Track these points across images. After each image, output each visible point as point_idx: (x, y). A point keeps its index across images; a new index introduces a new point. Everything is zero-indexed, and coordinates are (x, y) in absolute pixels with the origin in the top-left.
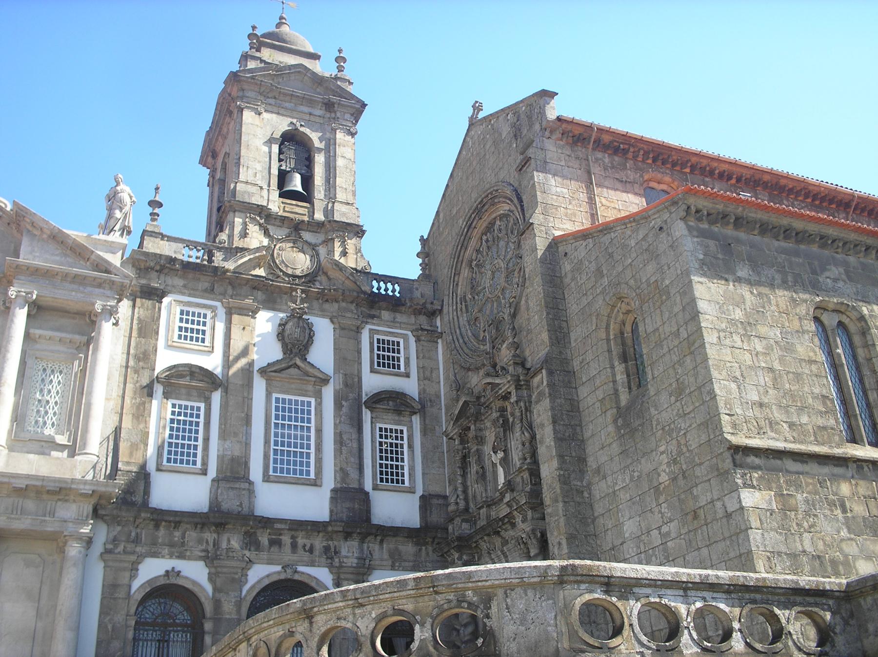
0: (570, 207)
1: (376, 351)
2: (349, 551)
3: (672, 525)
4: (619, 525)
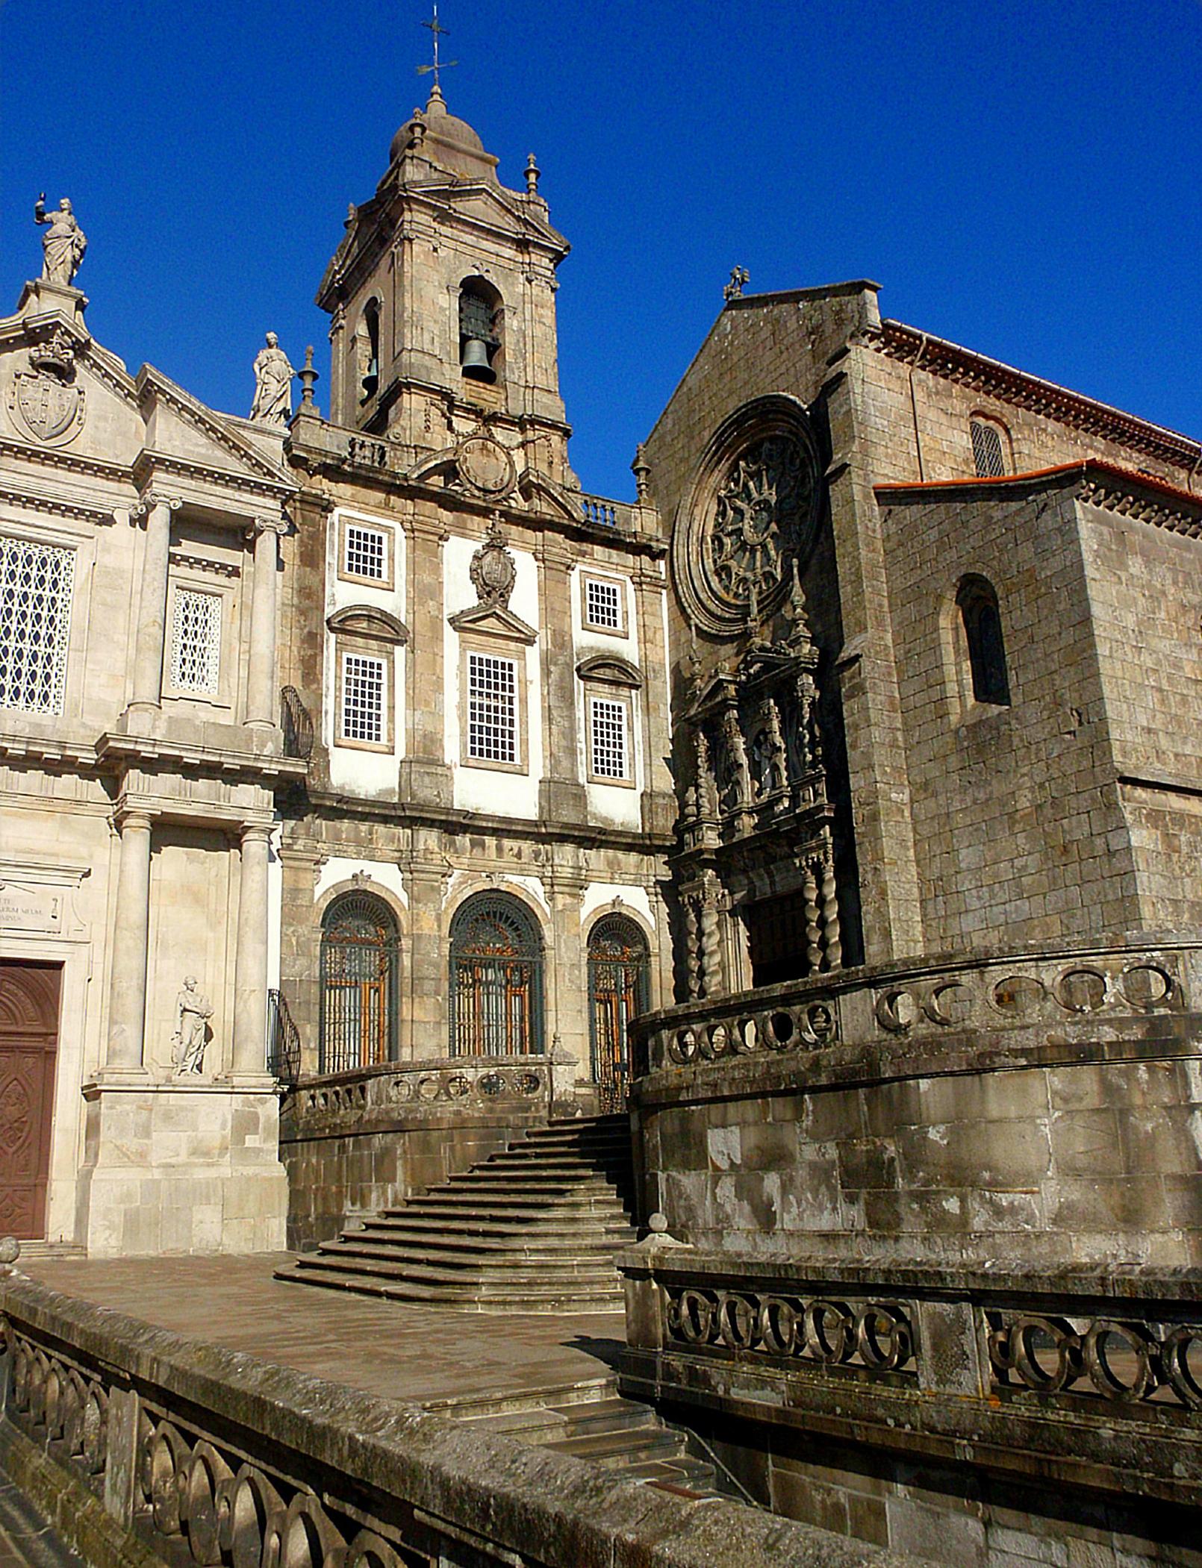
0: (890, 444)
1: (588, 602)
2: (566, 855)
3: (1030, 858)
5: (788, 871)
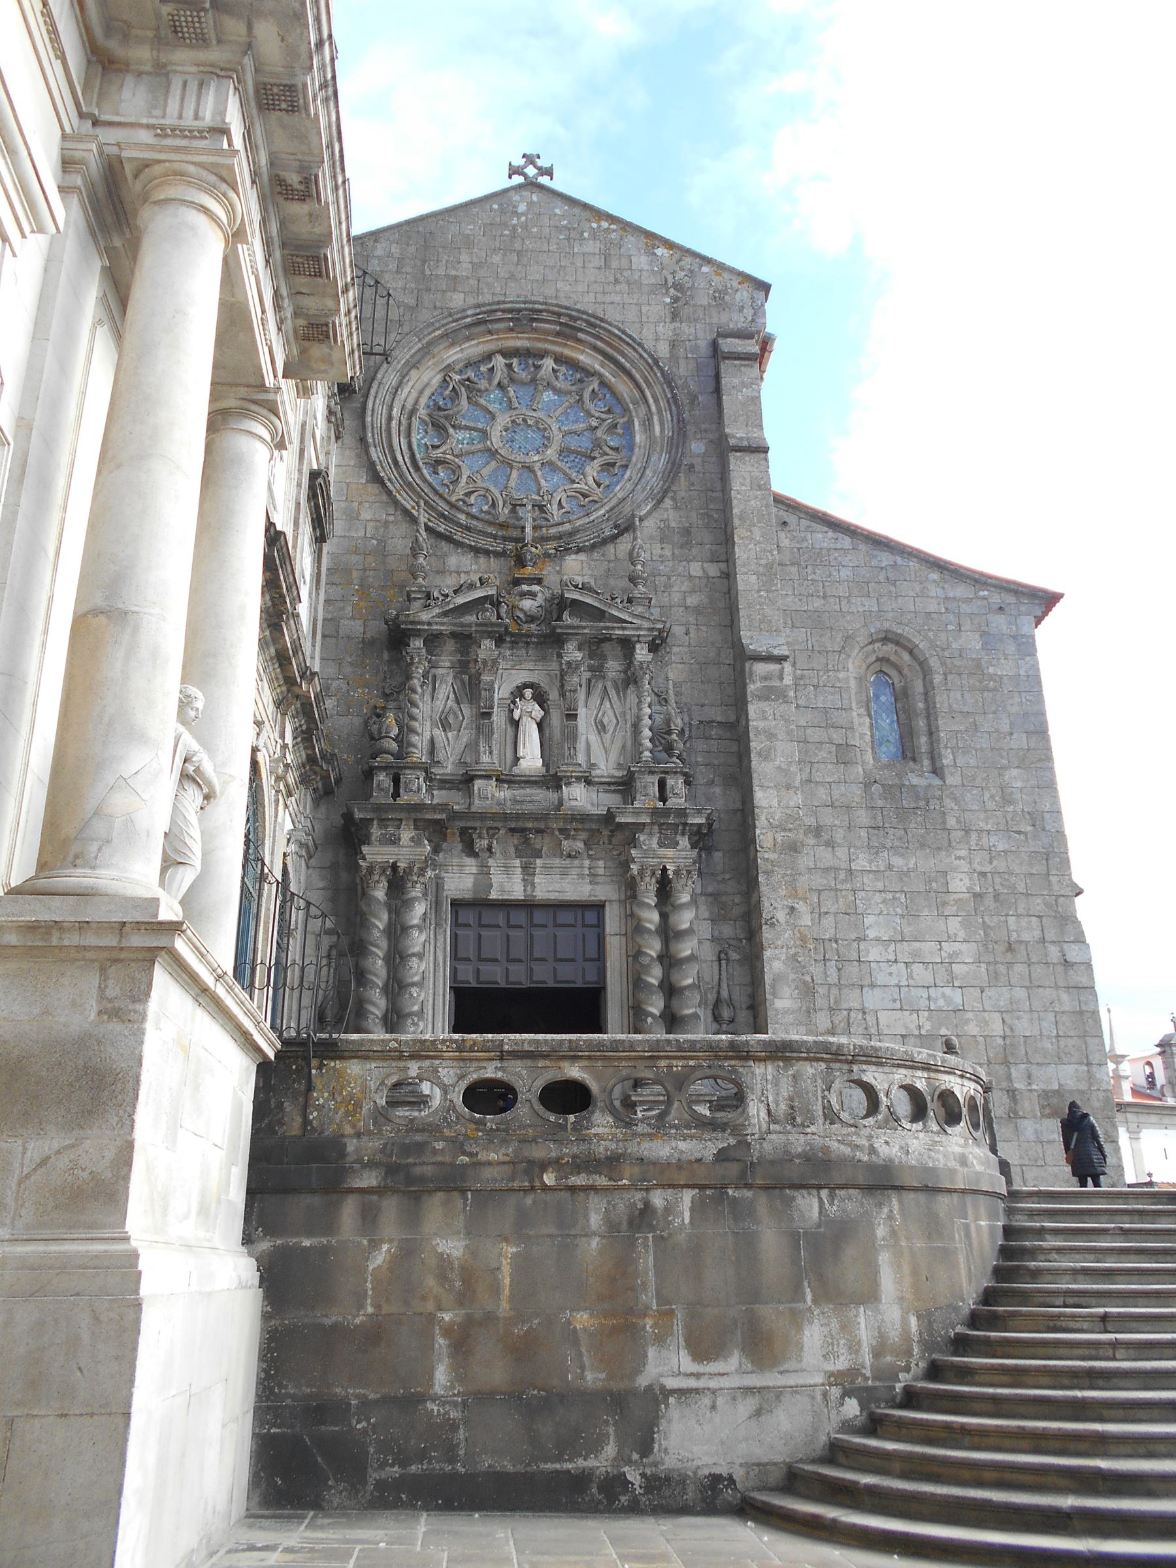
4: (852, 912)
5: (564, 874)
